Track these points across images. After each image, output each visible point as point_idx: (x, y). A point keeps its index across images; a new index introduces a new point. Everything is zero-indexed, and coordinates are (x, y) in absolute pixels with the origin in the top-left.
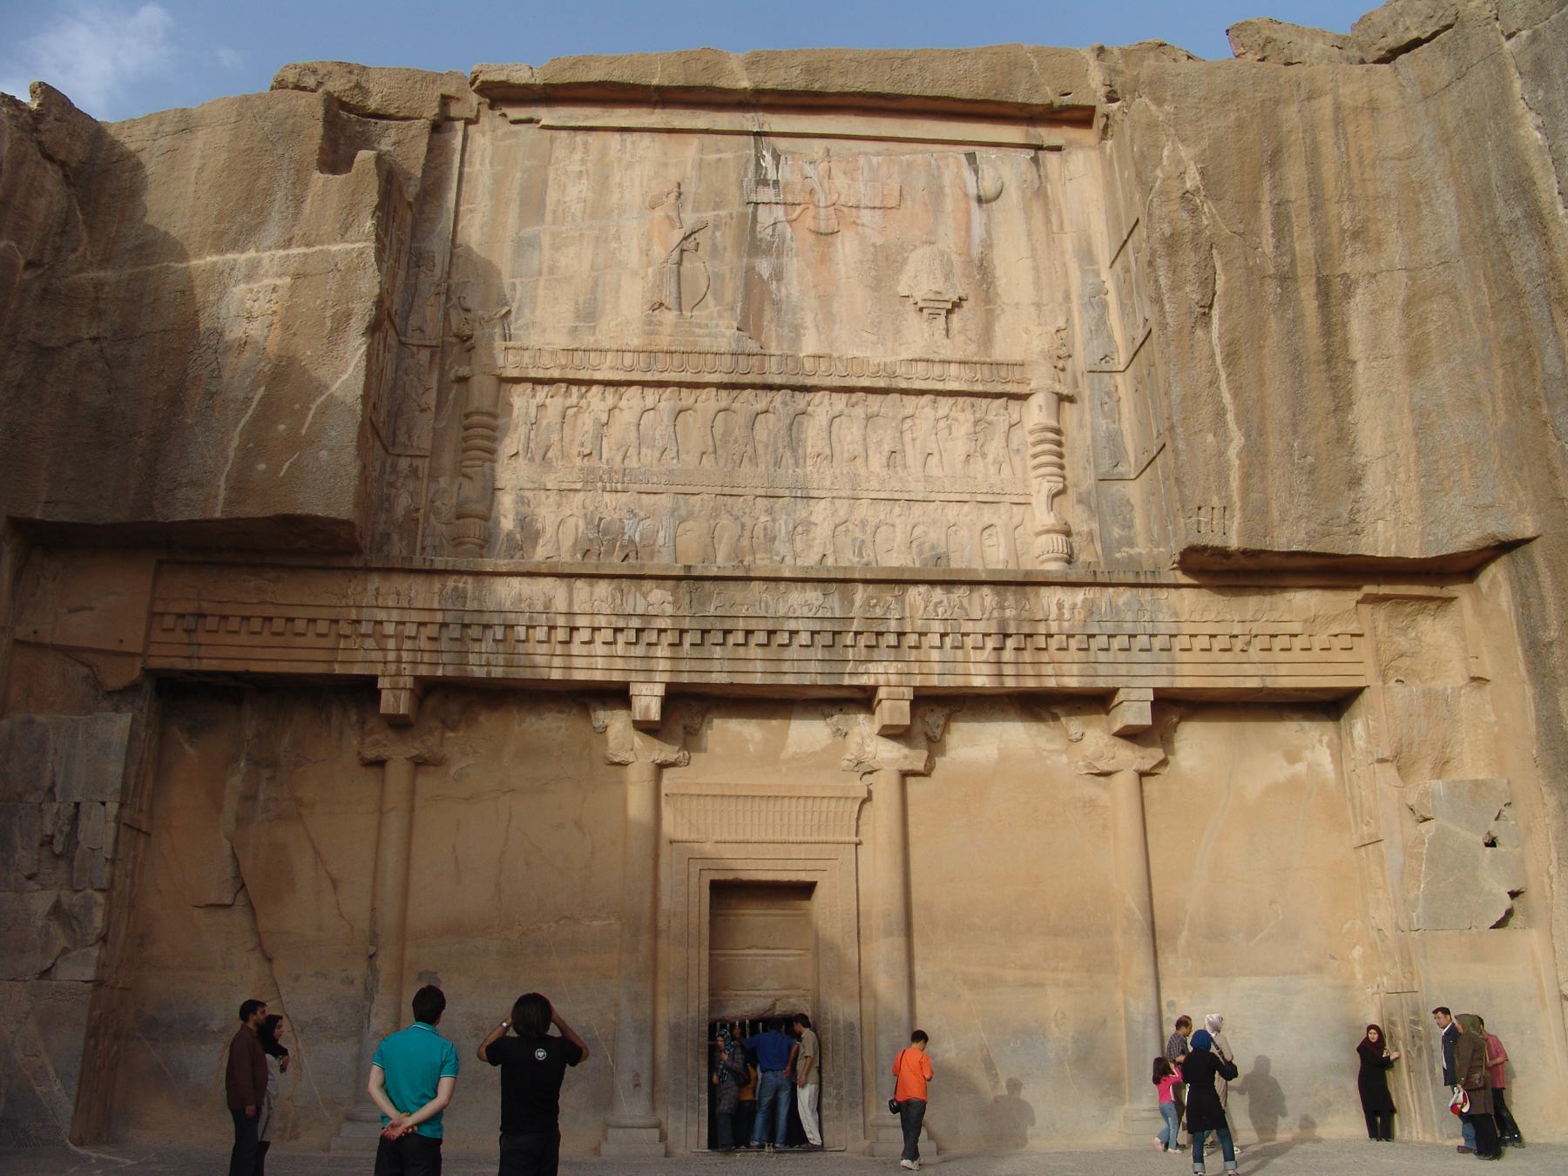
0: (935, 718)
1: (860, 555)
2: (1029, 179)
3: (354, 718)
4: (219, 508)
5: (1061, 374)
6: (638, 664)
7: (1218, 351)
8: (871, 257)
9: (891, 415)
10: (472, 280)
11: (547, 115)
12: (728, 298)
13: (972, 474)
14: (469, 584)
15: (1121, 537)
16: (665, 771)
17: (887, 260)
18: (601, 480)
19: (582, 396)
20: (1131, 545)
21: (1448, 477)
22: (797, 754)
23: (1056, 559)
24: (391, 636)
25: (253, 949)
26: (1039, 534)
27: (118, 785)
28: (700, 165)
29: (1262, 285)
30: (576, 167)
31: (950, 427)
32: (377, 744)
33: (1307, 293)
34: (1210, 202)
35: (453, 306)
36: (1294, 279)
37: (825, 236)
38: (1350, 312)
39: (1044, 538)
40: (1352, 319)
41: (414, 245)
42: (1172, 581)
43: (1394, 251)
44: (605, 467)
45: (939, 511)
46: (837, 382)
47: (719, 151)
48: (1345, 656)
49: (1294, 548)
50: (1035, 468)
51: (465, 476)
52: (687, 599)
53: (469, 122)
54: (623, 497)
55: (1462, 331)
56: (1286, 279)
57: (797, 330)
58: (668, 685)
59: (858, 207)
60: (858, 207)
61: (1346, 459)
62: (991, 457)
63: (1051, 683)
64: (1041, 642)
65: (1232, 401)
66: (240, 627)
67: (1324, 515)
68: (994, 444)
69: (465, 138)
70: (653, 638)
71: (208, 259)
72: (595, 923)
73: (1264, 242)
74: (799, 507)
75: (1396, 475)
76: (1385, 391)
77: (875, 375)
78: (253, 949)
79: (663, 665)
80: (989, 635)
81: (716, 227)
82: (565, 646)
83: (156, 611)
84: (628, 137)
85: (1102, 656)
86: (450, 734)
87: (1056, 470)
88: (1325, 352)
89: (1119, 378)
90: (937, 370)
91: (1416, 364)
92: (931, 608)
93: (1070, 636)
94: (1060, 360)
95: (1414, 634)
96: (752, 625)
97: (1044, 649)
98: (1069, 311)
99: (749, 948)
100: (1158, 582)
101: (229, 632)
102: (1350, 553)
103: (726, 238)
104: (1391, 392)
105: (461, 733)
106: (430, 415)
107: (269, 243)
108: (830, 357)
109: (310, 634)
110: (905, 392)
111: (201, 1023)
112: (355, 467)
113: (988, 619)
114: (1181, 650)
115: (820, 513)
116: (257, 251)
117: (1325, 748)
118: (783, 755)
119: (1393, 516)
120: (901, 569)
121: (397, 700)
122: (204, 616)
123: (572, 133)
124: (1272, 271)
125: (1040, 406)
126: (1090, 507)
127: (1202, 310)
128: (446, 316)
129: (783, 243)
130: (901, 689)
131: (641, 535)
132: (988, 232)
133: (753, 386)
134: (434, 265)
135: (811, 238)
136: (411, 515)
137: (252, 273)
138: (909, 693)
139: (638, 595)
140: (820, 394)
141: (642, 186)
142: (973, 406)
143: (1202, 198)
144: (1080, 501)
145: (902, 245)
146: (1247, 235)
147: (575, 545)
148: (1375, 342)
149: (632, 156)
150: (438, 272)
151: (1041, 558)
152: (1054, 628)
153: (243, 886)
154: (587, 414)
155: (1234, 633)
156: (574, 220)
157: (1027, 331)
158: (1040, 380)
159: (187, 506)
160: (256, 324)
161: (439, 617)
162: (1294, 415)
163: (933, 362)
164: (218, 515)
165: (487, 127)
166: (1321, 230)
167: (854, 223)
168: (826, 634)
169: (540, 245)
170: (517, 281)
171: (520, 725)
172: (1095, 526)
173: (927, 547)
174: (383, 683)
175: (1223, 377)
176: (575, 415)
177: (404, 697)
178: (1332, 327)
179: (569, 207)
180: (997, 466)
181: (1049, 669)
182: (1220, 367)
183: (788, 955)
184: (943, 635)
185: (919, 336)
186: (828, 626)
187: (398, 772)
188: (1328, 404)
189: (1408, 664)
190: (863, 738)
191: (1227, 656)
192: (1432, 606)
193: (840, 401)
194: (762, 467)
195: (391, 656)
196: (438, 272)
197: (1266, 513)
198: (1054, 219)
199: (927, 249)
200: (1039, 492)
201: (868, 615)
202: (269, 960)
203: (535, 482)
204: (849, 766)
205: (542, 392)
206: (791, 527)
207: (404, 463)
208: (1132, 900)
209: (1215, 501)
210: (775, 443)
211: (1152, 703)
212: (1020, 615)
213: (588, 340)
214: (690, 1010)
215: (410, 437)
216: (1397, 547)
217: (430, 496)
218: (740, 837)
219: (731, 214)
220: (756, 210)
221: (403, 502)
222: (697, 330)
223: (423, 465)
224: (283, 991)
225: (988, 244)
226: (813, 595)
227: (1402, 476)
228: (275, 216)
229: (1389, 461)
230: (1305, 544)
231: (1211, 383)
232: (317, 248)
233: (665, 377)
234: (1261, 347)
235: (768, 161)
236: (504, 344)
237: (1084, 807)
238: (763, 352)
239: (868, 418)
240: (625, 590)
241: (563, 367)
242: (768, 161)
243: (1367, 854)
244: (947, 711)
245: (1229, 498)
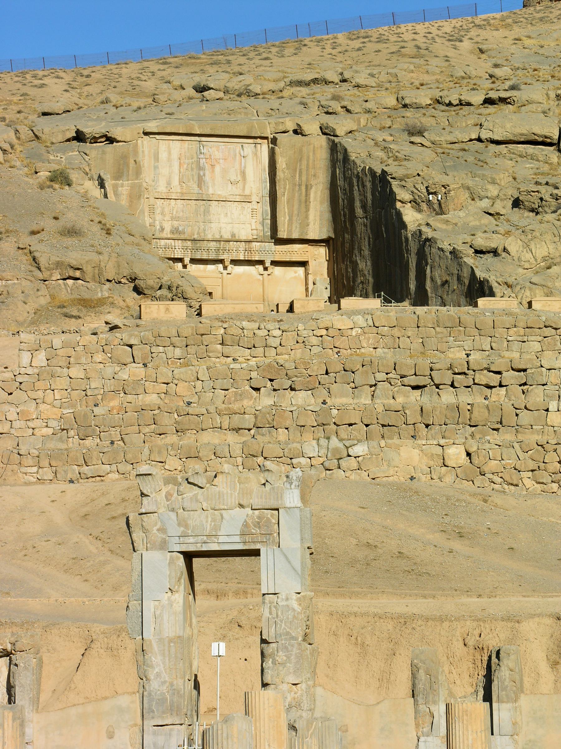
11: (158, 137)
12: (195, 180)
37: (213, 166)
56: (300, 185)
58: (191, 259)
103: (194, 166)
115: (212, 225)
135: (210, 166)
137: (122, 186)
146: (294, 177)
158: (254, 199)
166: (307, 175)
178: (307, 195)
188: (305, 210)
194: (202, 216)
225: (245, 167)
226: (214, 243)
235: (202, 148)
242: (202, 148)
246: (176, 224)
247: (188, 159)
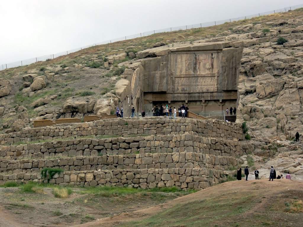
0: (207, 102)
14: (174, 94)
28: (189, 56)
30: (179, 57)
33: (234, 69)
37: (200, 63)
57: (197, 71)
94: (218, 73)
115: (199, 87)
137: (157, 73)
193: (201, 78)
225: (213, 62)
226: (198, 94)
239: (203, 79)
246: (183, 87)
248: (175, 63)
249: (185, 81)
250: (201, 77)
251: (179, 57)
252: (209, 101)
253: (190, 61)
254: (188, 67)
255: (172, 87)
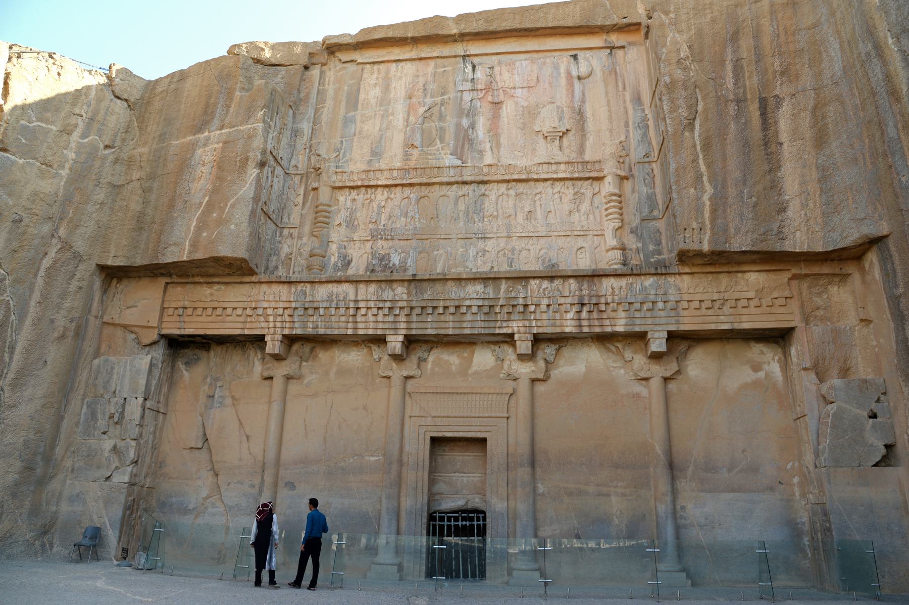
0: (549, 351)
1: (511, 266)
2: (607, 65)
3: (260, 356)
4: (185, 255)
5: (622, 165)
6: (391, 326)
7: (698, 143)
8: (520, 112)
9: (529, 193)
10: (322, 141)
11: (359, 56)
12: (447, 138)
13: (572, 221)
15: (654, 249)
16: (408, 380)
17: (529, 113)
18: (380, 235)
19: (372, 194)
20: (660, 253)
21: (840, 203)
22: (477, 371)
23: (617, 264)
24: (271, 315)
25: (210, 470)
26: (608, 251)
27: (143, 390)
28: (435, 74)
29: (726, 106)
31: (561, 198)
32: (268, 369)
34: (695, 63)
35: (313, 154)
36: (746, 100)
37: (497, 104)
38: (779, 116)
39: (610, 253)
40: (780, 120)
41: (295, 126)
42: (677, 271)
43: (807, 79)
44: (383, 228)
45: (554, 241)
46: (500, 178)
47: (445, 67)
48: (782, 310)
49: (744, 249)
50: (607, 216)
51: (315, 236)
52: (414, 292)
53: (323, 65)
54: (390, 243)
55: (846, 120)
56: (740, 101)
57: (481, 153)
58: (405, 336)
59: (514, 88)
60: (514, 88)
61: (776, 198)
62: (583, 211)
63: (609, 329)
64: (603, 307)
65: (706, 170)
66: (202, 313)
67: (762, 230)
68: (585, 204)
69: (322, 73)
70: (397, 312)
71: (188, 138)
72: (372, 459)
73: (727, 82)
74: (480, 243)
75: (807, 205)
76: (801, 158)
77: (520, 173)
78: (210, 470)
79: (403, 325)
80: (574, 304)
81: (442, 105)
82: (354, 317)
83: (165, 306)
84: (400, 65)
85: (637, 314)
86: (304, 364)
87: (617, 216)
88: (764, 139)
89: (654, 165)
90: (554, 167)
91: (820, 141)
92: (541, 291)
93: (618, 304)
95: (826, 296)
96: (448, 303)
97: (604, 311)
98: (628, 131)
99: (455, 473)
100: (668, 272)
101: (197, 315)
102: (778, 250)
104: (805, 159)
105: (310, 363)
106: (299, 207)
107: (214, 128)
108: (497, 165)
109: (234, 315)
110: (537, 180)
111: (185, 505)
112: (247, 232)
113: (573, 296)
114: (683, 309)
115: (490, 245)
116: (209, 132)
117: (777, 364)
118: (470, 372)
119: (806, 228)
120: (535, 271)
121: (274, 346)
122: (185, 308)
123: (372, 65)
124: (732, 97)
125: (609, 183)
126: (637, 235)
127: (688, 122)
128: (309, 159)
129: (476, 109)
130: (526, 335)
131: (400, 260)
132: (583, 94)
133: (457, 183)
134: (304, 135)
136: (289, 257)
138: (531, 337)
139: (390, 290)
140: (492, 184)
141: (406, 88)
142: (573, 185)
143: (691, 62)
144: (632, 232)
145: (537, 106)
147: (367, 267)
148: (795, 133)
149: (402, 73)
150: (305, 138)
151: (609, 263)
152: (610, 300)
153: (207, 439)
154: (374, 203)
155: (714, 299)
156: (372, 108)
157: (604, 144)
159: (172, 255)
160: (206, 167)
161: (293, 305)
162: (745, 175)
163: (551, 163)
164: (185, 258)
165: (332, 66)
167: (512, 96)
168: (486, 307)
169: (355, 121)
170: (344, 140)
171: (338, 358)
172: (640, 245)
173: (547, 260)
174: (268, 338)
175: (701, 156)
176: (369, 203)
177: (277, 344)
179: (370, 102)
180: (586, 216)
181: (607, 322)
182: (700, 152)
183: (474, 477)
184: (548, 306)
185: (544, 151)
186: (486, 303)
187: (278, 382)
189: (822, 313)
190: (511, 362)
191: (710, 312)
192: (837, 279)
193: (503, 187)
194: (461, 224)
195: (271, 325)
196: (305, 138)
197: (726, 230)
198: (620, 84)
199: (551, 106)
200: (608, 228)
201: (508, 296)
202: (217, 475)
203: (348, 237)
204: (503, 377)
205: (354, 193)
206: (475, 254)
207: (286, 232)
208: (659, 449)
209: (695, 225)
210: (468, 211)
211: (667, 340)
212: (590, 293)
213: (376, 166)
214: (418, 504)
215: (289, 219)
216: (808, 245)
217: (298, 246)
218: (446, 415)
219: (449, 98)
220: (462, 94)
221: (285, 249)
222: (429, 157)
223: (295, 232)
224: (222, 490)
225: (583, 101)
226: (479, 287)
227: (811, 205)
228: (218, 115)
229: (803, 197)
230: (750, 247)
231: (693, 161)
232: (236, 128)
233: (413, 181)
234: (725, 139)
236: (334, 169)
237: (634, 397)
238: (462, 165)
239: (516, 195)
240: (384, 288)
241: (362, 180)
243: (800, 423)
244: (557, 346)
245: (704, 223)
246: (382, 246)
247: (432, 97)
248: (342, 110)
249: (397, 211)
250: (508, 181)
251: (372, 79)
252: (560, 340)
253: (439, 99)
254: (423, 131)
255: (306, 251)
